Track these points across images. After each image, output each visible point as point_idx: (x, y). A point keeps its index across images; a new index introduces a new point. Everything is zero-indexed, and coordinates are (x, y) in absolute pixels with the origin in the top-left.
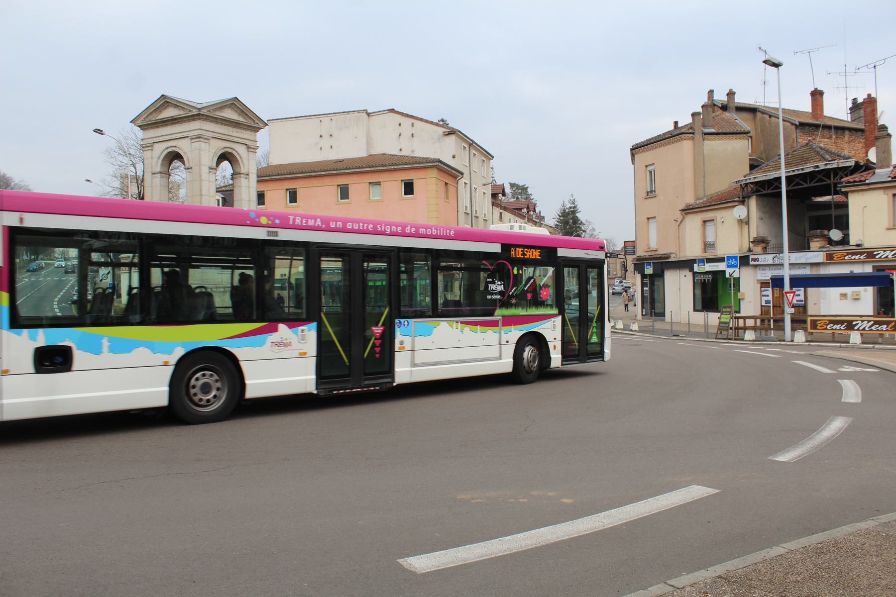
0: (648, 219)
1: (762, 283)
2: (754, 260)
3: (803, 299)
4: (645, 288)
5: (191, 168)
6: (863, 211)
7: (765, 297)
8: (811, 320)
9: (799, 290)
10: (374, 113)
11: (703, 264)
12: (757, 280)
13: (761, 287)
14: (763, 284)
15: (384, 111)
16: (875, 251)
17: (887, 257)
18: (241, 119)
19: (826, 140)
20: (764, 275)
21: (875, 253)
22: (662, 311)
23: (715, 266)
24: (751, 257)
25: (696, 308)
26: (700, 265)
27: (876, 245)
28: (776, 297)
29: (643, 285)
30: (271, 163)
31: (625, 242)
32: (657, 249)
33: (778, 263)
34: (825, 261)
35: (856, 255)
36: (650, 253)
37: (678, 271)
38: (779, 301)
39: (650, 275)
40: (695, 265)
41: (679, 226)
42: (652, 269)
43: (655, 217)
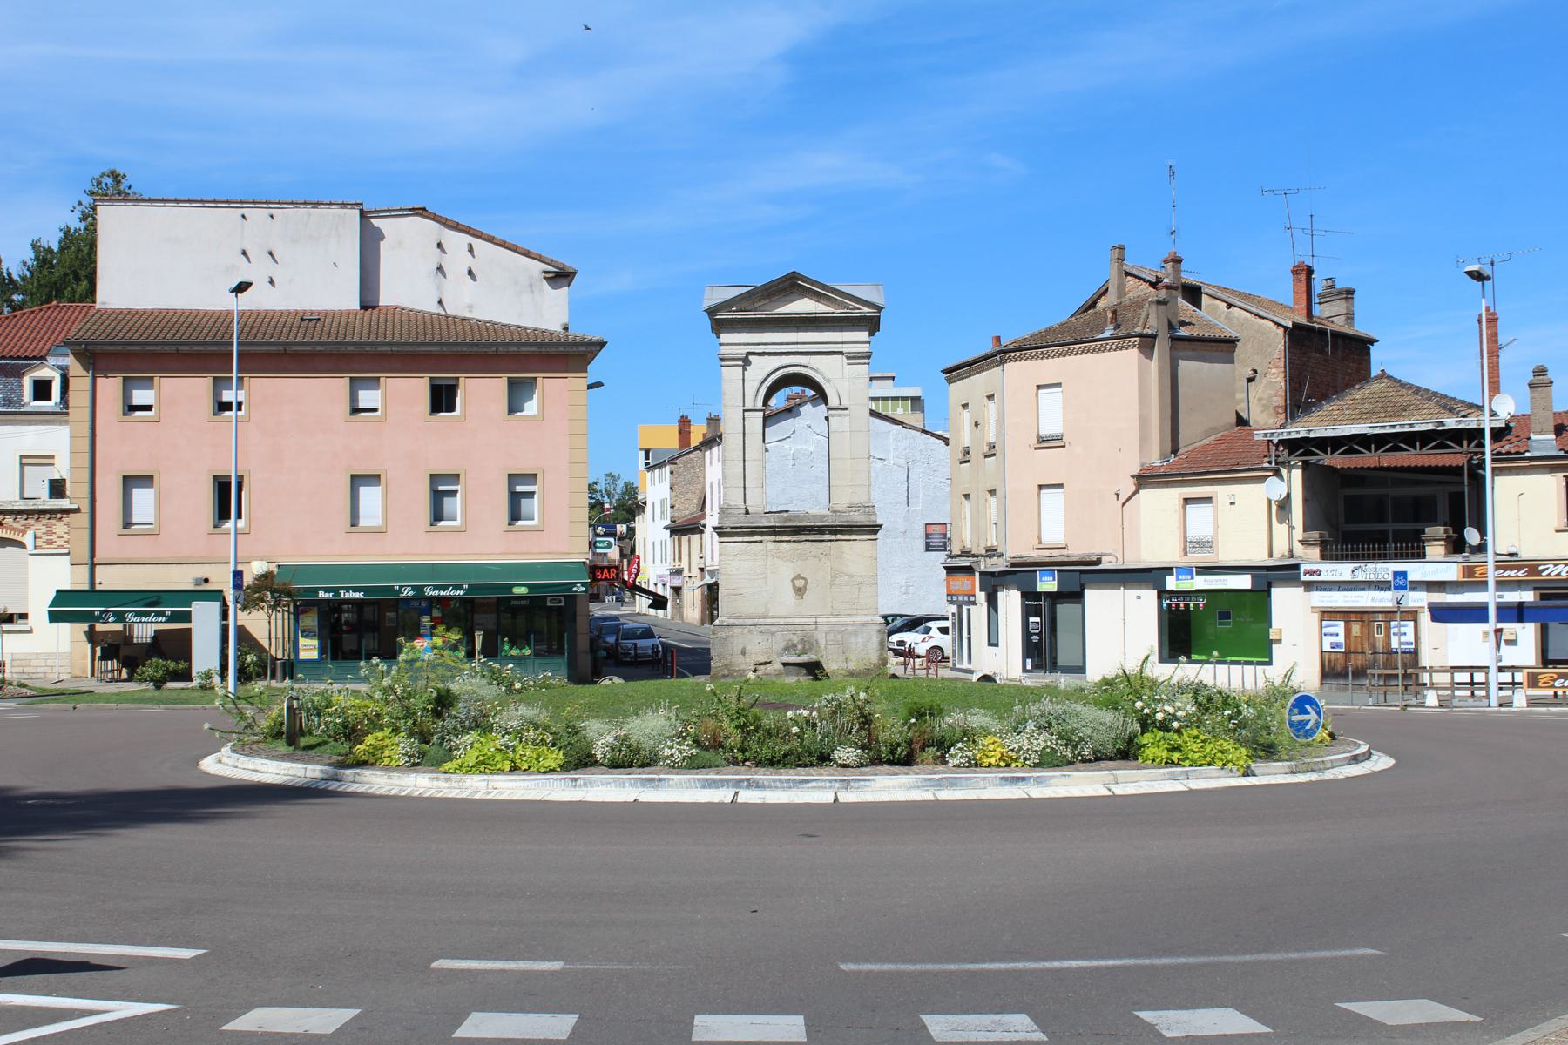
0: (1041, 487)
1: (1324, 612)
2: (1312, 573)
3: (1412, 640)
4: (1031, 619)
5: (846, 409)
6: (1518, 500)
7: (1330, 637)
8: (1528, 673)
9: (1405, 626)
10: (376, 211)
11: (1189, 577)
12: (1312, 607)
13: (1322, 621)
14: (1326, 615)
15: (401, 210)
16: (1541, 565)
17: (1559, 574)
18: (838, 312)
19: (1317, 355)
20: (1329, 599)
21: (1541, 568)
23: (1217, 581)
24: (1303, 568)
25: (1551, 656)
26: (1181, 577)
27: (1537, 555)
28: (1356, 637)
29: (1027, 612)
30: (104, 303)
31: (927, 524)
33: (1364, 579)
34: (1461, 579)
35: (1511, 570)
37: (1122, 588)
38: (1362, 644)
39: (1048, 595)
41: (1124, 504)
42: (1056, 582)
43: (1060, 486)
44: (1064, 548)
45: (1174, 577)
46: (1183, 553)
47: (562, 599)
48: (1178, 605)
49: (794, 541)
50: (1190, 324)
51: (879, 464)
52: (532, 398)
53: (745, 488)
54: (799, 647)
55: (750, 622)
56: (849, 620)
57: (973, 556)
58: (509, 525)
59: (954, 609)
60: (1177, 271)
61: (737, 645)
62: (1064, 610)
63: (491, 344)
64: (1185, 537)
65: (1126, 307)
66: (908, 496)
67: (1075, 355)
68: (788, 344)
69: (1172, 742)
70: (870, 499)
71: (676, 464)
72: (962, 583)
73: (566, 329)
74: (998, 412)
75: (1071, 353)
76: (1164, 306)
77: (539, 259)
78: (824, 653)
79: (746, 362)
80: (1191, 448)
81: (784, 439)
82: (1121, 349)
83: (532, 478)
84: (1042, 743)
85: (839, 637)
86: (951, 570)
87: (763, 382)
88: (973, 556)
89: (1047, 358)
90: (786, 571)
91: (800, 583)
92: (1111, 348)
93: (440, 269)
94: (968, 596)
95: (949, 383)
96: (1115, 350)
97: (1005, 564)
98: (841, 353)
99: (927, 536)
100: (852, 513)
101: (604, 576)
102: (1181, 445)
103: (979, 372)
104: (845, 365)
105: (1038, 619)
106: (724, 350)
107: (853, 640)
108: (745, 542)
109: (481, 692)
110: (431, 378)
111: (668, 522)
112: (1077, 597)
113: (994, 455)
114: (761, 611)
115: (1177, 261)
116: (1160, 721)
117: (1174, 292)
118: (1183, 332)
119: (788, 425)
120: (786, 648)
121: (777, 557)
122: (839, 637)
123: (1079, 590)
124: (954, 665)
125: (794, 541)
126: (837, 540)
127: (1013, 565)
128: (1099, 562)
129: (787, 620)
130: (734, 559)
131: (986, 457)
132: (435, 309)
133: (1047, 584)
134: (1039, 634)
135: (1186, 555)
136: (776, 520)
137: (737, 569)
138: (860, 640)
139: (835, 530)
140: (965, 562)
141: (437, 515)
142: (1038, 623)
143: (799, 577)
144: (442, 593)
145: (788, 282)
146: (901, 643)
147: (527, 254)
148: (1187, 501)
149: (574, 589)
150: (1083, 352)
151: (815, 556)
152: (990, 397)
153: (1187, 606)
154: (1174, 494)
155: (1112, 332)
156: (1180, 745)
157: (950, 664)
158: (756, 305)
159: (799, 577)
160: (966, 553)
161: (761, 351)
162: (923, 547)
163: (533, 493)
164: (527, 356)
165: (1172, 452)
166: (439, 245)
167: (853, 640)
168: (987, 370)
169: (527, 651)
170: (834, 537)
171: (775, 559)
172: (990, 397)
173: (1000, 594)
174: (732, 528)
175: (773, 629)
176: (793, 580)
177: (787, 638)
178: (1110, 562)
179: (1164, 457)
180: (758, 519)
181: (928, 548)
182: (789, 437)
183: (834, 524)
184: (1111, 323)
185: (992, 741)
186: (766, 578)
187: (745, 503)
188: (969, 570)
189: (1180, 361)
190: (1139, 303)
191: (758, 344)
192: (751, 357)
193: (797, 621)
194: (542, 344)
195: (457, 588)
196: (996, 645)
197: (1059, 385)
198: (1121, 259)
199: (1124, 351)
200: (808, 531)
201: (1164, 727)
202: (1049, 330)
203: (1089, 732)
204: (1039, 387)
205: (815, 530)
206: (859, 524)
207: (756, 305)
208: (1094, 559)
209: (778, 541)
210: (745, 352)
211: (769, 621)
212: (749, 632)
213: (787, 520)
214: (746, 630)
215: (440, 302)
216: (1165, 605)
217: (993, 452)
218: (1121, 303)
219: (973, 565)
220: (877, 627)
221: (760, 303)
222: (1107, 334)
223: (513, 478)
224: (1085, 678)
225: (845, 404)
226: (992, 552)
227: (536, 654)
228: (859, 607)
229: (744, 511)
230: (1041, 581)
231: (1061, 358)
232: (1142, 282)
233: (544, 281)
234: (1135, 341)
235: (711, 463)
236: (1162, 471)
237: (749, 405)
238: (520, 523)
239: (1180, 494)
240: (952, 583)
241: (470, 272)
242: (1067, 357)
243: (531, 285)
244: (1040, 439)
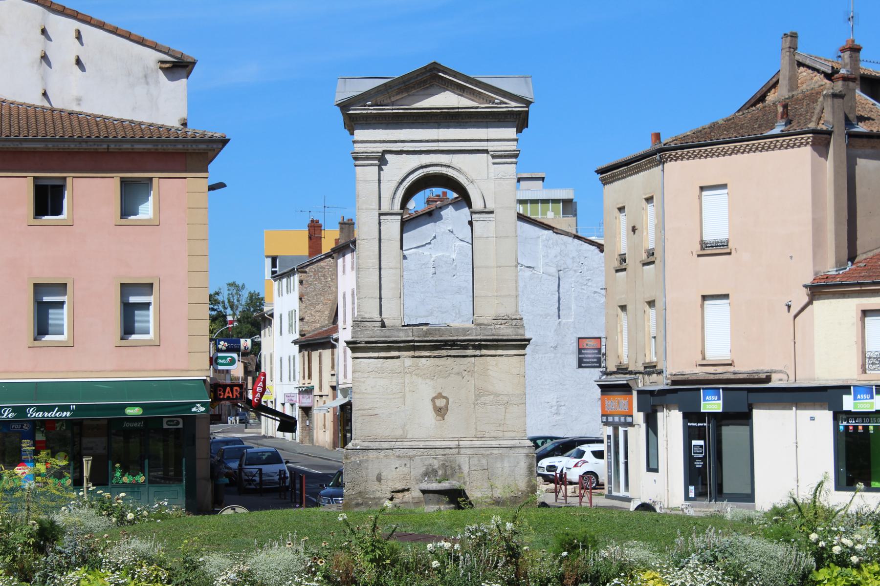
0: (704, 298)
4: (694, 442)
5: (492, 212)
22: (749, 492)
26: (859, 397)
29: (690, 434)
31: (579, 338)
32: (733, 361)
36: (711, 369)
37: (794, 408)
39: (713, 415)
40: (844, 397)
41: (795, 316)
42: (721, 402)
43: (726, 296)
44: (731, 365)
45: (852, 397)
46: (861, 370)
47: (181, 420)
48: (856, 428)
49: (435, 357)
50: (869, 119)
51: (528, 272)
52: (147, 200)
53: (380, 298)
54: (440, 473)
55: (385, 445)
56: (494, 443)
57: (631, 373)
58: (122, 339)
59: (609, 431)
60: (855, 61)
61: (372, 471)
62: (730, 433)
63: (102, 141)
64: (864, 353)
65: (799, 101)
66: (559, 309)
67: (742, 153)
68: (428, 141)
69: (850, 579)
70: (517, 311)
71: (306, 272)
72: (617, 402)
73: (185, 124)
74: (657, 216)
75: (738, 151)
76: (840, 100)
77: (155, 47)
78: (467, 479)
79: (382, 161)
80: (870, 255)
81: (424, 245)
82: (793, 147)
83: (148, 288)
84: (706, 579)
85: (484, 461)
86: (606, 389)
87: (401, 183)
88: (631, 373)
89: (711, 157)
90: (426, 390)
91: (441, 403)
92: (782, 146)
93: (45, 57)
94: (626, 416)
95: (604, 184)
96: (786, 148)
97: (665, 381)
98: (486, 151)
99: (580, 351)
100: (497, 327)
101: (227, 395)
102: (858, 252)
103: (637, 173)
104: (490, 164)
105: (701, 443)
106: (359, 148)
107: (499, 465)
108: (381, 358)
109: (89, 524)
110: (35, 178)
111: (297, 336)
112: (745, 418)
113: (653, 262)
114: (398, 433)
115: (855, 50)
116: (837, 555)
117: (851, 84)
118: (862, 128)
119: (428, 229)
120: (426, 474)
121: (416, 375)
122: (484, 461)
123: (747, 411)
124: (610, 492)
125: (435, 357)
126: (481, 356)
127: (674, 383)
128: (768, 379)
129: (427, 443)
130: (369, 377)
131: (644, 264)
132: (39, 101)
133: (712, 404)
134: (703, 459)
135: (864, 371)
136: (415, 333)
137: (372, 387)
138: (506, 464)
139: (480, 345)
140: (621, 380)
141: (42, 329)
142: (701, 446)
143: (440, 396)
144: (46, 414)
145: (428, 74)
146: (552, 468)
147: (141, 42)
148: (865, 313)
149: (194, 409)
150: (750, 150)
151: (458, 374)
152: (649, 200)
153: (866, 428)
154: (851, 306)
155: (783, 128)
156: (859, 582)
157: (606, 492)
158: (393, 99)
159: (440, 396)
160: (622, 370)
161: (399, 149)
162: (575, 363)
163: (148, 304)
164: (141, 154)
165: (849, 259)
166: (44, 31)
167: (499, 465)
168: (645, 170)
169: (141, 478)
170: (478, 352)
171: (414, 377)
172: (649, 200)
173: (660, 415)
174: (367, 343)
175: (411, 453)
176: (433, 400)
177: (427, 463)
178: (781, 380)
179: (840, 265)
180: (396, 333)
181: (581, 364)
182: (429, 243)
183: (479, 338)
184: (782, 118)
185: (651, 577)
186: (404, 397)
187: (381, 314)
188: (626, 389)
189: (858, 160)
190: (812, 97)
191: (395, 142)
192: (388, 156)
193: (438, 444)
194: (159, 141)
195: (63, 409)
196: (656, 470)
197: (724, 186)
198: (793, 48)
199: (796, 149)
200: (450, 345)
201: (842, 561)
202: (714, 127)
203: (758, 567)
204: (702, 189)
205: (457, 345)
206: (505, 338)
207: (393, 99)
208: (763, 376)
209: (417, 357)
210: (381, 150)
211: (407, 444)
212: (386, 456)
213: (427, 333)
214: (382, 454)
215: (45, 94)
216: (841, 428)
217: (651, 259)
218: (793, 96)
219: (630, 383)
220: (526, 451)
221: (399, 97)
222: (777, 131)
223: (126, 288)
224: (754, 506)
225: (490, 207)
226: (651, 369)
227: (151, 481)
228: (506, 429)
229: (379, 324)
230: (704, 400)
231: (727, 157)
232: (816, 73)
233: (161, 73)
234: (809, 138)
235: (344, 272)
236: (838, 281)
237: (385, 208)
238: (134, 337)
239: (857, 306)
240: (607, 402)
241: (78, 62)
242: (734, 156)
243: (146, 77)
244: (704, 245)
